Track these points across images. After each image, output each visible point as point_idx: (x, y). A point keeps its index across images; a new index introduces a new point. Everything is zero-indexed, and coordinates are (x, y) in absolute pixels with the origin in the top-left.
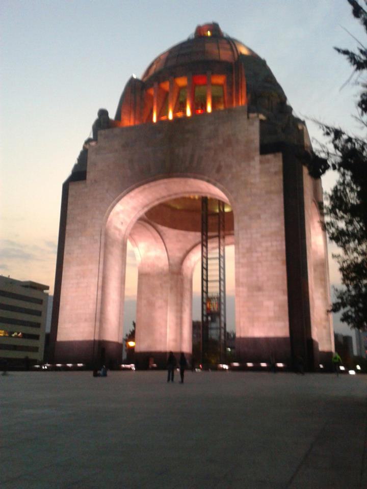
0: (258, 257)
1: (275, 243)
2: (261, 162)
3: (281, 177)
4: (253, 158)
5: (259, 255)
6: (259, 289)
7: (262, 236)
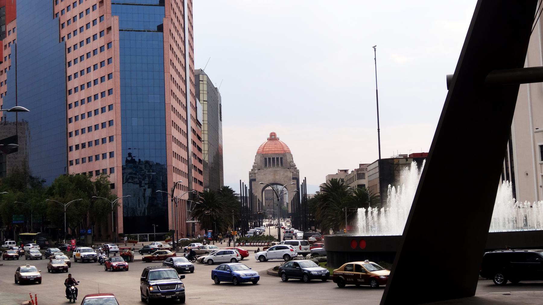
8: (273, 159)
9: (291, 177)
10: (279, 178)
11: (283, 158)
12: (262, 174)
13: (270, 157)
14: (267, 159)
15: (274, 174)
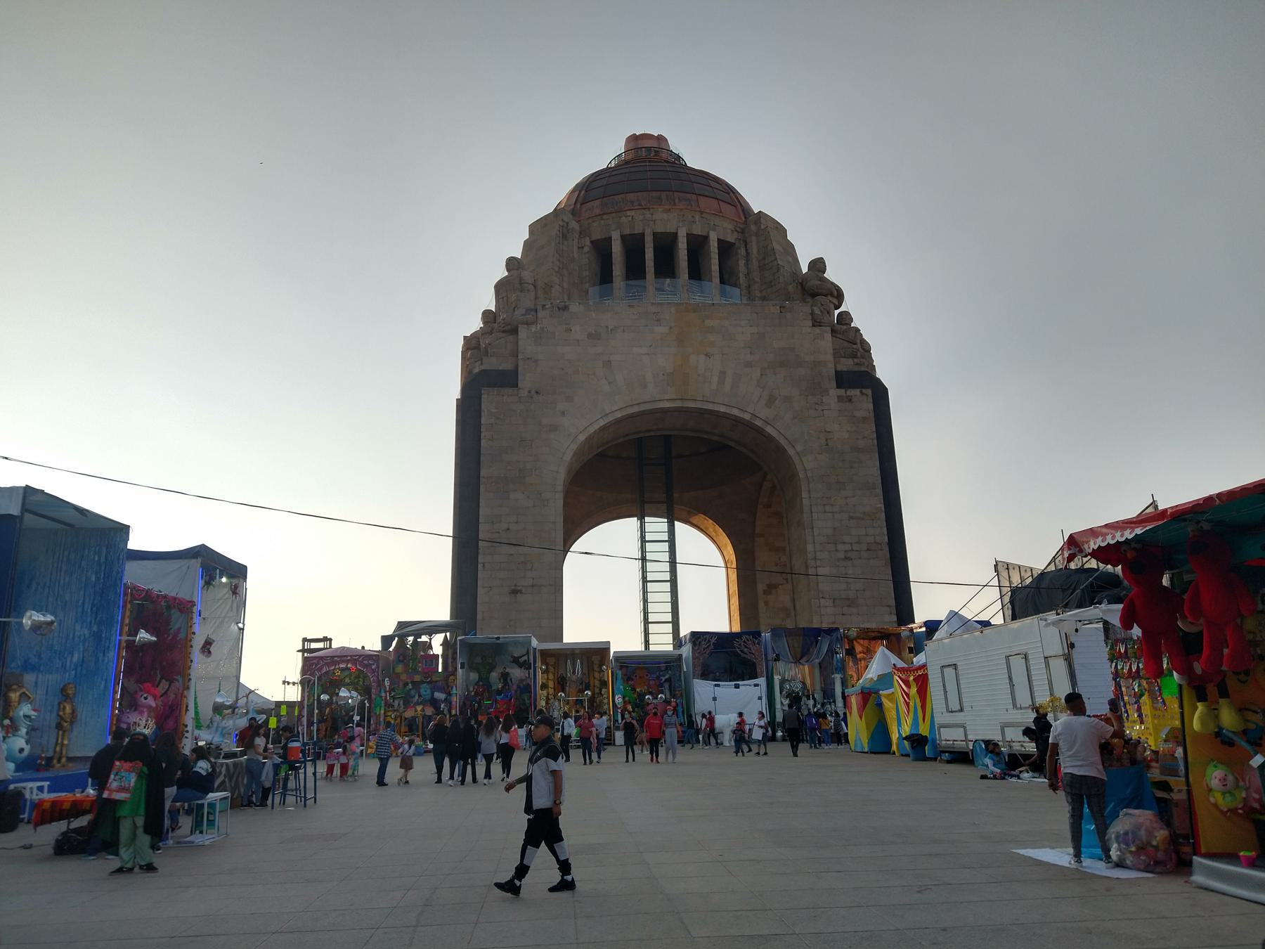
2: (840, 399)
5: (848, 547)
7: (851, 518)
8: (665, 247)
10: (723, 373)
11: (742, 252)
14: (617, 248)
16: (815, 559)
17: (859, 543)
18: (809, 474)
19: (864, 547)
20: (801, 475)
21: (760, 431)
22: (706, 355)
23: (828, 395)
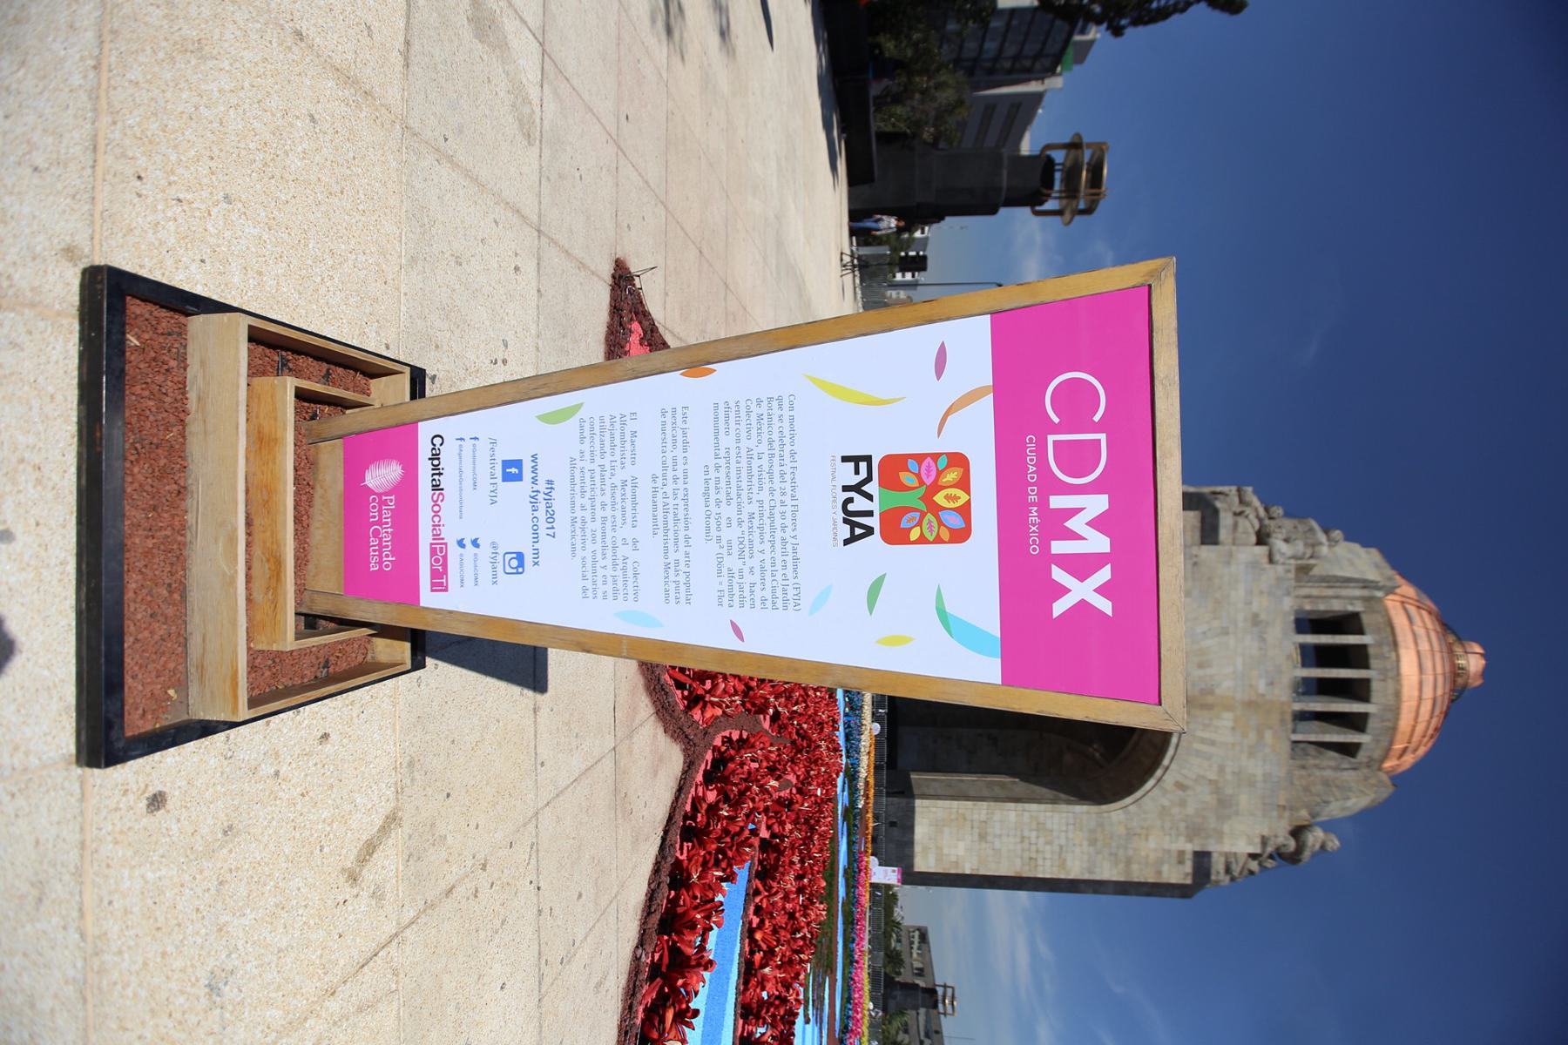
0: (1029, 838)
1: (1048, 863)
2: (1181, 853)
3: (1151, 880)
4: (1190, 839)
5: (1033, 840)
6: (983, 837)
7: (1061, 847)
9: (1220, 835)
10: (1213, 743)
12: (1260, 604)
13: (1373, 662)
15: (1251, 705)
16: (1024, 810)
17: (1037, 851)
18: (1105, 815)
19: (1034, 855)
20: (1104, 807)
21: (1150, 772)
22: (1233, 729)
23: (1187, 842)
